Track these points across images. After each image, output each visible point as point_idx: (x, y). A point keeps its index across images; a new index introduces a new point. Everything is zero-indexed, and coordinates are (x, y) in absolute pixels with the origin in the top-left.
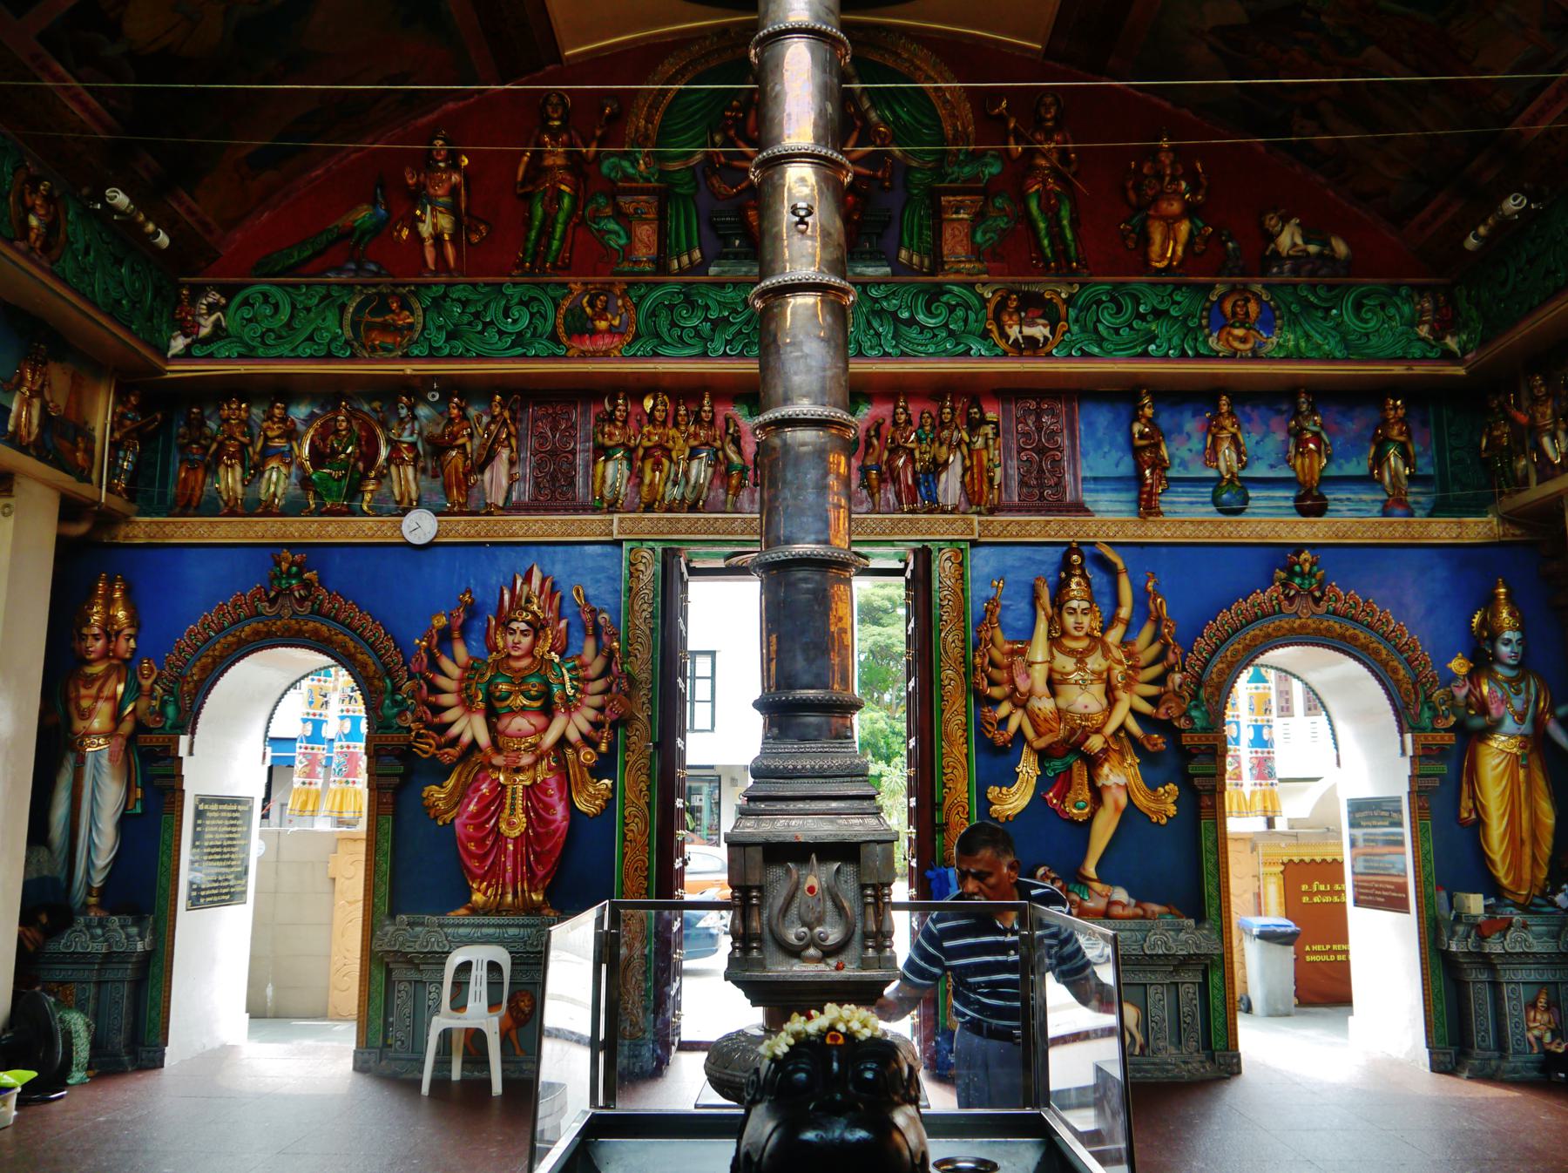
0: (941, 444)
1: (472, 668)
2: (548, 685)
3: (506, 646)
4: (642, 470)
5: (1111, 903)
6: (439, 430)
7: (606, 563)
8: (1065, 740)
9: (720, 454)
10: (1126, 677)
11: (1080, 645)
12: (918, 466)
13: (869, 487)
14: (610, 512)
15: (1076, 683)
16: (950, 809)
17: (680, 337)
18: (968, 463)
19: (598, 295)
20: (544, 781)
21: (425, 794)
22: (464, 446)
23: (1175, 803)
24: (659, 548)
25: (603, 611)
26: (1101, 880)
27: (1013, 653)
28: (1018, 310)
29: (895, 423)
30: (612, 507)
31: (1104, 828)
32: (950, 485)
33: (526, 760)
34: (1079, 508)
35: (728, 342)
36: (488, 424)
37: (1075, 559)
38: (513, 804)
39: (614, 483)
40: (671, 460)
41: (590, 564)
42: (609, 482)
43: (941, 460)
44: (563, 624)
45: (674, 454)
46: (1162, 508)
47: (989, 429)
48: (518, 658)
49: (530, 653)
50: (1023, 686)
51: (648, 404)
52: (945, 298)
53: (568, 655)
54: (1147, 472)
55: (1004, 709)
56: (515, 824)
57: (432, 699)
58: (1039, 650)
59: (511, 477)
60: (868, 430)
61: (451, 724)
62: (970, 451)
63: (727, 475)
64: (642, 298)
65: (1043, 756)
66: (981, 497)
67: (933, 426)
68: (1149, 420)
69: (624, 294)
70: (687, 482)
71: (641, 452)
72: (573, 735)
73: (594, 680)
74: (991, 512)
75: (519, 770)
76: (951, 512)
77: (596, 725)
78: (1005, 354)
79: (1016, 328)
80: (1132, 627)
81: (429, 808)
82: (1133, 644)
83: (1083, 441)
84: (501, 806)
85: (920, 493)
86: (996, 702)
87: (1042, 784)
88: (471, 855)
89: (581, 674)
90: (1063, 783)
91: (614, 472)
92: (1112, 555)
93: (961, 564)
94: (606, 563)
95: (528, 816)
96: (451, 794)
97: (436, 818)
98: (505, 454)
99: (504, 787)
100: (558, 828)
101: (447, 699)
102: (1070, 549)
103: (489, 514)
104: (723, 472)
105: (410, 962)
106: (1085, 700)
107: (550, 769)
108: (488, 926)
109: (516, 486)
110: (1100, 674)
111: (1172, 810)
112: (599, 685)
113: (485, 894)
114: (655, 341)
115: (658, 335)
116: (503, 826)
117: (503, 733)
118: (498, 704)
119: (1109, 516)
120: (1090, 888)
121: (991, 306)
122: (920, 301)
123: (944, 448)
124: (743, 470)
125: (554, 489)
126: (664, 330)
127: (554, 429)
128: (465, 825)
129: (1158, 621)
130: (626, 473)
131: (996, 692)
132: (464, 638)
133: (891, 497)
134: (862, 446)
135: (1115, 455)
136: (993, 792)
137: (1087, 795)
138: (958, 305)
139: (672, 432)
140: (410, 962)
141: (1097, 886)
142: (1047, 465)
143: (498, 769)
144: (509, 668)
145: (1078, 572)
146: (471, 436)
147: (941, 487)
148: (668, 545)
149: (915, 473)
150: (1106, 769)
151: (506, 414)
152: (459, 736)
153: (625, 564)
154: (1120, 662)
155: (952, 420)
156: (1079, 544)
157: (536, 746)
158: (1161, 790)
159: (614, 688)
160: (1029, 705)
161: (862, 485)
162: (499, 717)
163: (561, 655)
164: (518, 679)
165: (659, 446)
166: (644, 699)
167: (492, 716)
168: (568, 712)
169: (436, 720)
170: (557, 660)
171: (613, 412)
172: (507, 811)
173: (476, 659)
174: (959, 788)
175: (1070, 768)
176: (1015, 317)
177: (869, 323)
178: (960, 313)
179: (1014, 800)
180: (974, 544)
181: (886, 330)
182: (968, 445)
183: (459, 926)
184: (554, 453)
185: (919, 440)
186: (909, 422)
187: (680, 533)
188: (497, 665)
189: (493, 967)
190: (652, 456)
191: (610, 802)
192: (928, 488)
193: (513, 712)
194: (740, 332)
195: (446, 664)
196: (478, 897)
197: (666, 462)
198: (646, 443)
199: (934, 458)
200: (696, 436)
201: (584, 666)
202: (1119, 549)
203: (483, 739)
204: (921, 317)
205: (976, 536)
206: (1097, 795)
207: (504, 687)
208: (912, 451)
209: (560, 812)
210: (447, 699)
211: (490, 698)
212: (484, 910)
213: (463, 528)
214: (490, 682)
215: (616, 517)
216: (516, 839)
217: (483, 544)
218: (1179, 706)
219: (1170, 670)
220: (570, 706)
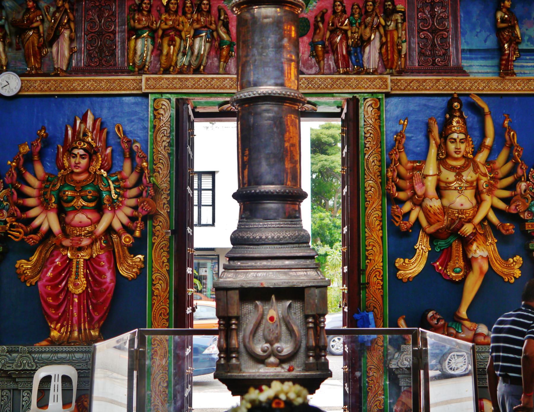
0: (366, 27)
1: (48, 181)
2: (99, 192)
3: (70, 166)
4: (161, 45)
5: (476, 335)
6: (20, 17)
7: (137, 109)
8: (448, 227)
9: (215, 34)
10: (489, 184)
11: (458, 164)
12: (350, 42)
13: (316, 56)
14: (140, 74)
15: (456, 189)
16: (370, 273)
18: (384, 40)
20: (98, 256)
21: (17, 266)
22: (37, 28)
23: (520, 268)
24: (173, 98)
25: (136, 141)
26: (470, 319)
27: (413, 169)
29: (334, 12)
30: (141, 70)
31: (472, 286)
32: (372, 55)
33: (85, 242)
34: (459, 71)
36: (54, 13)
37: (457, 105)
38: (77, 272)
39: (142, 54)
40: (181, 38)
41: (126, 109)
42: (139, 53)
43: (366, 37)
44: (109, 150)
45: (183, 34)
46: (516, 70)
47: (398, 17)
48: (79, 174)
49: (86, 170)
50: (420, 191)
53: (113, 171)
54: (506, 45)
55: (407, 207)
56: (79, 285)
57: (21, 201)
58: (431, 167)
59: (71, 50)
60: (316, 17)
61: (34, 218)
62: (385, 31)
63: (220, 48)
65: (433, 238)
66: (392, 64)
67: (360, 15)
68: (508, 9)
70: (192, 53)
71: (160, 32)
72: (117, 225)
73: (130, 188)
74: (400, 73)
75: (81, 249)
76: (373, 74)
77: (132, 219)
80: (494, 152)
81: (20, 274)
82: (494, 163)
83: (463, 25)
84: (69, 273)
86: (402, 202)
87: (432, 256)
88: (49, 305)
89: (122, 184)
90: (446, 255)
91: (142, 46)
92: (481, 103)
93: (379, 109)
94: (137, 109)
95: (87, 280)
96: (35, 266)
97: (25, 281)
98: (67, 33)
99: (71, 260)
100: (108, 287)
101: (31, 202)
102: (452, 98)
103: (57, 75)
104: (217, 46)
105: (10, 376)
106: (461, 200)
107: (102, 248)
108: (62, 352)
109: (75, 56)
110: (472, 182)
111: (518, 273)
112: (134, 192)
113: (59, 331)
116: (71, 286)
117: (69, 224)
118: (65, 205)
119: (479, 76)
120: (463, 325)
123: (368, 30)
124: (231, 45)
125: (102, 59)
127: (100, 17)
128: (45, 286)
129: (511, 147)
130: (151, 47)
131: (402, 195)
132: (42, 160)
133: (332, 63)
134: (312, 28)
135: (484, 34)
136: (399, 262)
137: (462, 263)
140: (10, 376)
141: (467, 324)
142: (438, 41)
143: (66, 248)
144: (73, 180)
145: (458, 114)
146: (42, 21)
147: (366, 56)
148: (180, 96)
149: (348, 47)
150: (474, 247)
151: (67, 6)
152: (40, 226)
153: (150, 109)
154: (485, 175)
155: (373, 10)
156: (459, 95)
157: (92, 233)
158: (511, 260)
159: (144, 194)
160: (424, 204)
161: (312, 55)
162: (66, 213)
163: (108, 171)
164: (79, 188)
165: (172, 28)
166: (165, 201)
167: (62, 213)
168: (114, 210)
169: (24, 216)
170: (105, 175)
171: (140, 5)
172: (73, 277)
173: (50, 175)
174: (376, 259)
175: (451, 246)
179: (413, 267)
180: (388, 95)
182: (384, 27)
183: (42, 352)
184: (100, 34)
185: (351, 24)
186: (344, 11)
187: (188, 88)
188: (64, 179)
189: (66, 379)
190: (168, 35)
191: (142, 271)
192: (357, 57)
193: (76, 210)
195: (30, 178)
196: (54, 334)
197: (177, 39)
198: (164, 26)
199: (361, 36)
200: (198, 21)
201: (124, 179)
202: (486, 98)
203: (56, 228)
205: (389, 90)
206: (469, 264)
207: (69, 193)
208: (346, 31)
209: (109, 276)
210: (31, 202)
211: (60, 201)
212: (59, 342)
213: (39, 85)
214: (60, 190)
215: (144, 77)
216: (79, 295)
217: (53, 96)
218: (524, 204)
219: (518, 180)
220: (115, 206)
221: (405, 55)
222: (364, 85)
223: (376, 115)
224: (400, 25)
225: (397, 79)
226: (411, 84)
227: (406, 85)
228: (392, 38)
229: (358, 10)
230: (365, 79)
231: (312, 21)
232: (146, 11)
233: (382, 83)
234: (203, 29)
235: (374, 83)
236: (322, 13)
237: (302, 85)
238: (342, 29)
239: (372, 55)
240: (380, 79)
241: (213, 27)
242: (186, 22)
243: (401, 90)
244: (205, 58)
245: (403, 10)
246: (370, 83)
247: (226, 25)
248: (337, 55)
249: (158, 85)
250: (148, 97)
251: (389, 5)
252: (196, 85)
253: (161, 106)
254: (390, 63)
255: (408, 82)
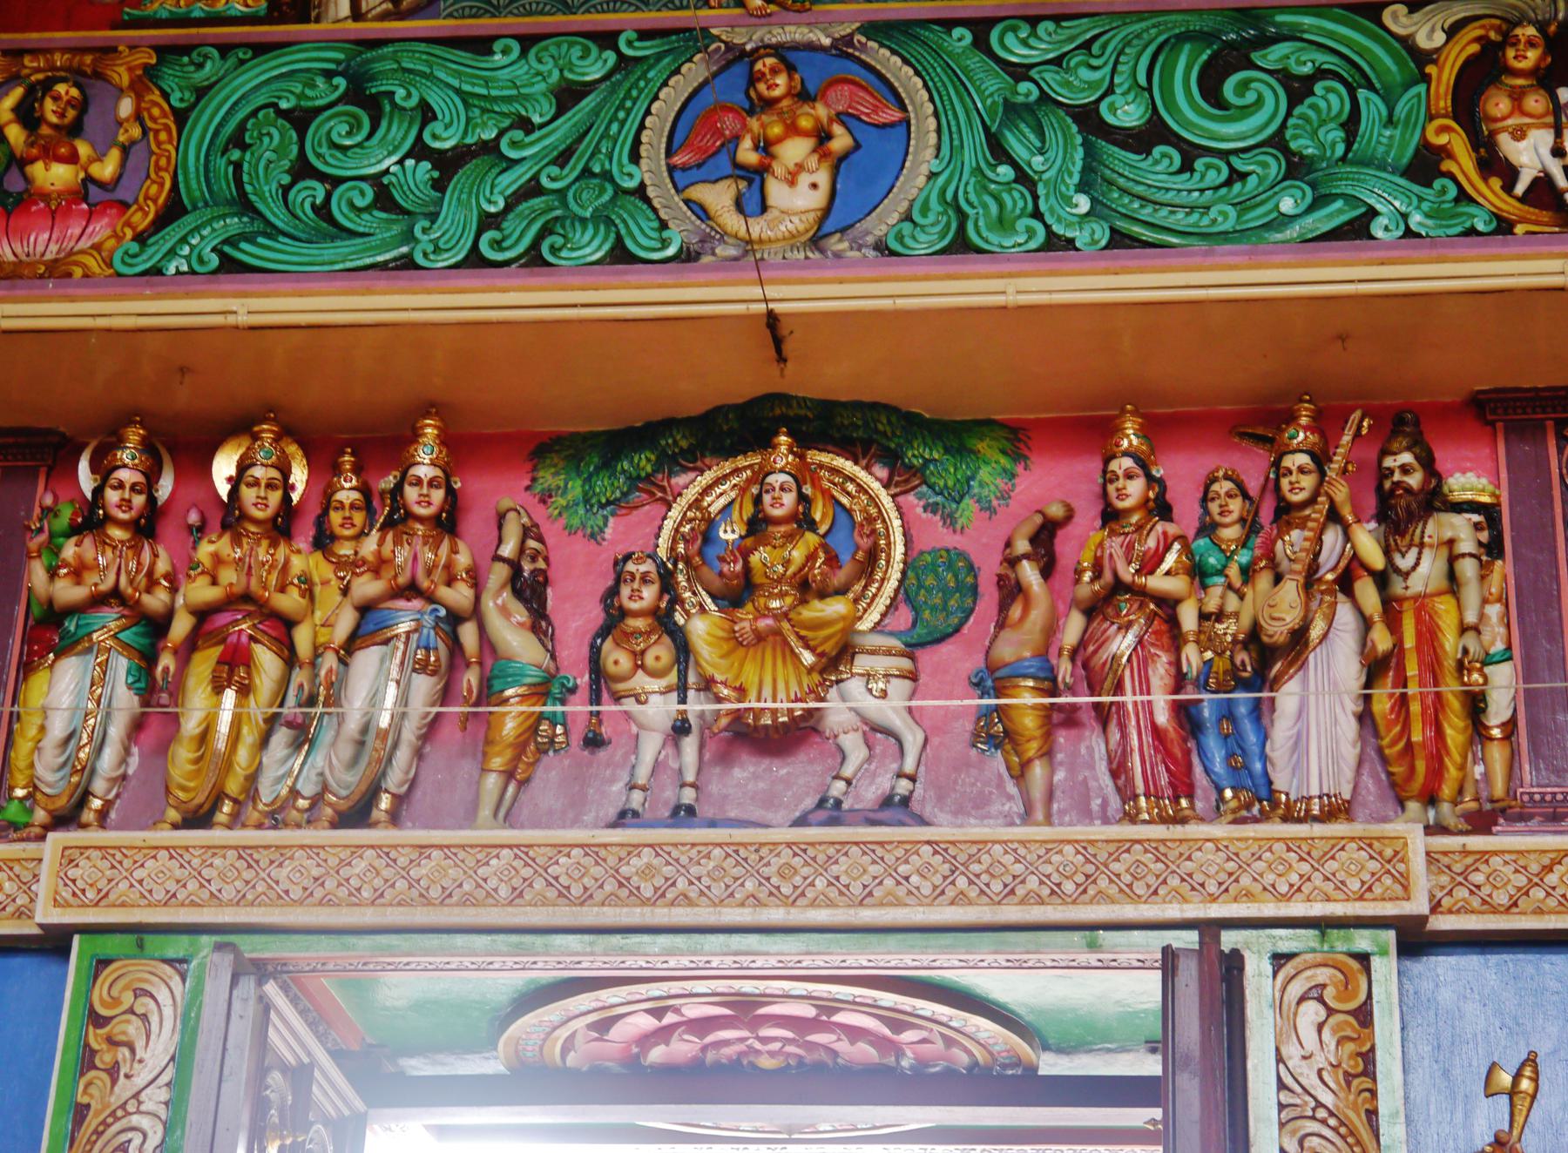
0: (1278, 579)
4: (177, 690)
9: (468, 634)
12: (1192, 657)
17: (323, 211)
18: (1382, 640)
19: (47, 86)
28: (1547, 79)
29: (1111, 516)
32: (1316, 723)
35: (489, 222)
43: (1277, 632)
45: (303, 638)
47: (1462, 530)
51: (224, 466)
52: (1273, 56)
64: (201, 92)
67: (1250, 525)
69: (145, 80)
71: (181, 626)
74: (1481, 822)
78: (1504, 227)
79: (1542, 139)
85: (1203, 758)
93: (1364, 1015)
114: (234, 224)
115: (244, 205)
121: (1445, 75)
122: (1185, 67)
126: (265, 189)
134: (989, 597)
138: (1321, 74)
139: (304, 561)
147: (1282, 730)
165: (242, 600)
176: (1536, 102)
177: (999, 152)
178: (1329, 99)
180: (1416, 940)
181: (1055, 157)
182: (1382, 580)
186: (1161, 508)
187: (283, 898)
190: (220, 637)
194: (533, 189)
197: (267, 660)
199: (1255, 632)
200: (379, 566)
204: (1190, 116)
205: (1418, 905)
208: (1168, 605)
221: (1510, 727)
222: (1270, 878)
223: (1350, 1047)
224: (1468, 568)
225: (1465, 852)
226: (1552, 879)
227: (1521, 880)
228: (1429, 635)
229: (1236, 505)
230: (1279, 847)
231: (990, 567)
232: (122, 524)
233: (1373, 866)
234: (401, 603)
235: (1332, 866)
236: (1038, 519)
237: (915, 879)
238: (1141, 593)
239: (1316, 723)
240: (1367, 842)
241: (460, 595)
242: (325, 583)
243: (1490, 908)
244: (403, 756)
245: (1486, 499)
246: (1305, 868)
247: (530, 591)
248: (1123, 727)
249: (124, 885)
250: (63, 952)
251: (1405, 469)
252: (330, 884)
253: (128, 998)
254: (1421, 766)
255: (1534, 868)
